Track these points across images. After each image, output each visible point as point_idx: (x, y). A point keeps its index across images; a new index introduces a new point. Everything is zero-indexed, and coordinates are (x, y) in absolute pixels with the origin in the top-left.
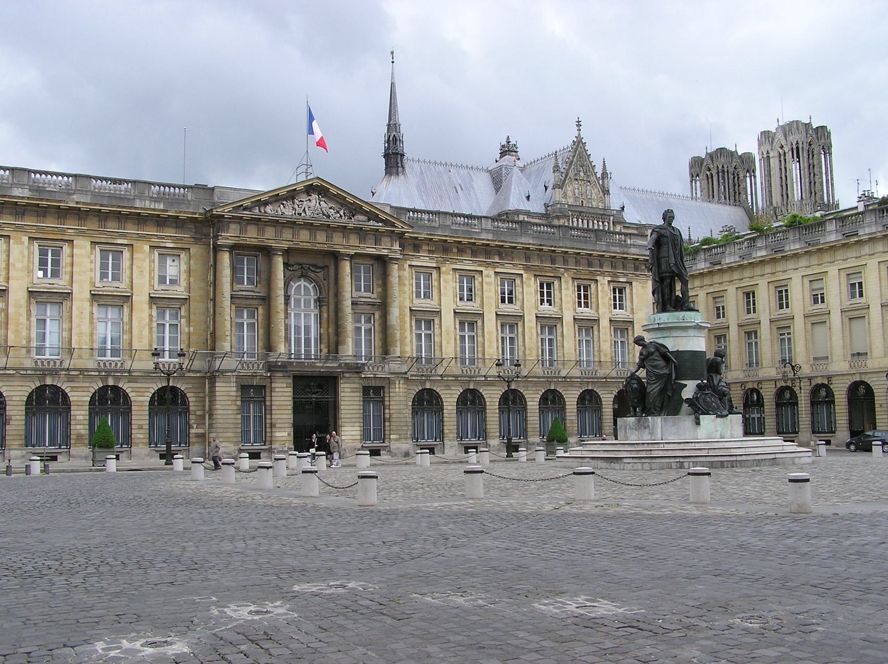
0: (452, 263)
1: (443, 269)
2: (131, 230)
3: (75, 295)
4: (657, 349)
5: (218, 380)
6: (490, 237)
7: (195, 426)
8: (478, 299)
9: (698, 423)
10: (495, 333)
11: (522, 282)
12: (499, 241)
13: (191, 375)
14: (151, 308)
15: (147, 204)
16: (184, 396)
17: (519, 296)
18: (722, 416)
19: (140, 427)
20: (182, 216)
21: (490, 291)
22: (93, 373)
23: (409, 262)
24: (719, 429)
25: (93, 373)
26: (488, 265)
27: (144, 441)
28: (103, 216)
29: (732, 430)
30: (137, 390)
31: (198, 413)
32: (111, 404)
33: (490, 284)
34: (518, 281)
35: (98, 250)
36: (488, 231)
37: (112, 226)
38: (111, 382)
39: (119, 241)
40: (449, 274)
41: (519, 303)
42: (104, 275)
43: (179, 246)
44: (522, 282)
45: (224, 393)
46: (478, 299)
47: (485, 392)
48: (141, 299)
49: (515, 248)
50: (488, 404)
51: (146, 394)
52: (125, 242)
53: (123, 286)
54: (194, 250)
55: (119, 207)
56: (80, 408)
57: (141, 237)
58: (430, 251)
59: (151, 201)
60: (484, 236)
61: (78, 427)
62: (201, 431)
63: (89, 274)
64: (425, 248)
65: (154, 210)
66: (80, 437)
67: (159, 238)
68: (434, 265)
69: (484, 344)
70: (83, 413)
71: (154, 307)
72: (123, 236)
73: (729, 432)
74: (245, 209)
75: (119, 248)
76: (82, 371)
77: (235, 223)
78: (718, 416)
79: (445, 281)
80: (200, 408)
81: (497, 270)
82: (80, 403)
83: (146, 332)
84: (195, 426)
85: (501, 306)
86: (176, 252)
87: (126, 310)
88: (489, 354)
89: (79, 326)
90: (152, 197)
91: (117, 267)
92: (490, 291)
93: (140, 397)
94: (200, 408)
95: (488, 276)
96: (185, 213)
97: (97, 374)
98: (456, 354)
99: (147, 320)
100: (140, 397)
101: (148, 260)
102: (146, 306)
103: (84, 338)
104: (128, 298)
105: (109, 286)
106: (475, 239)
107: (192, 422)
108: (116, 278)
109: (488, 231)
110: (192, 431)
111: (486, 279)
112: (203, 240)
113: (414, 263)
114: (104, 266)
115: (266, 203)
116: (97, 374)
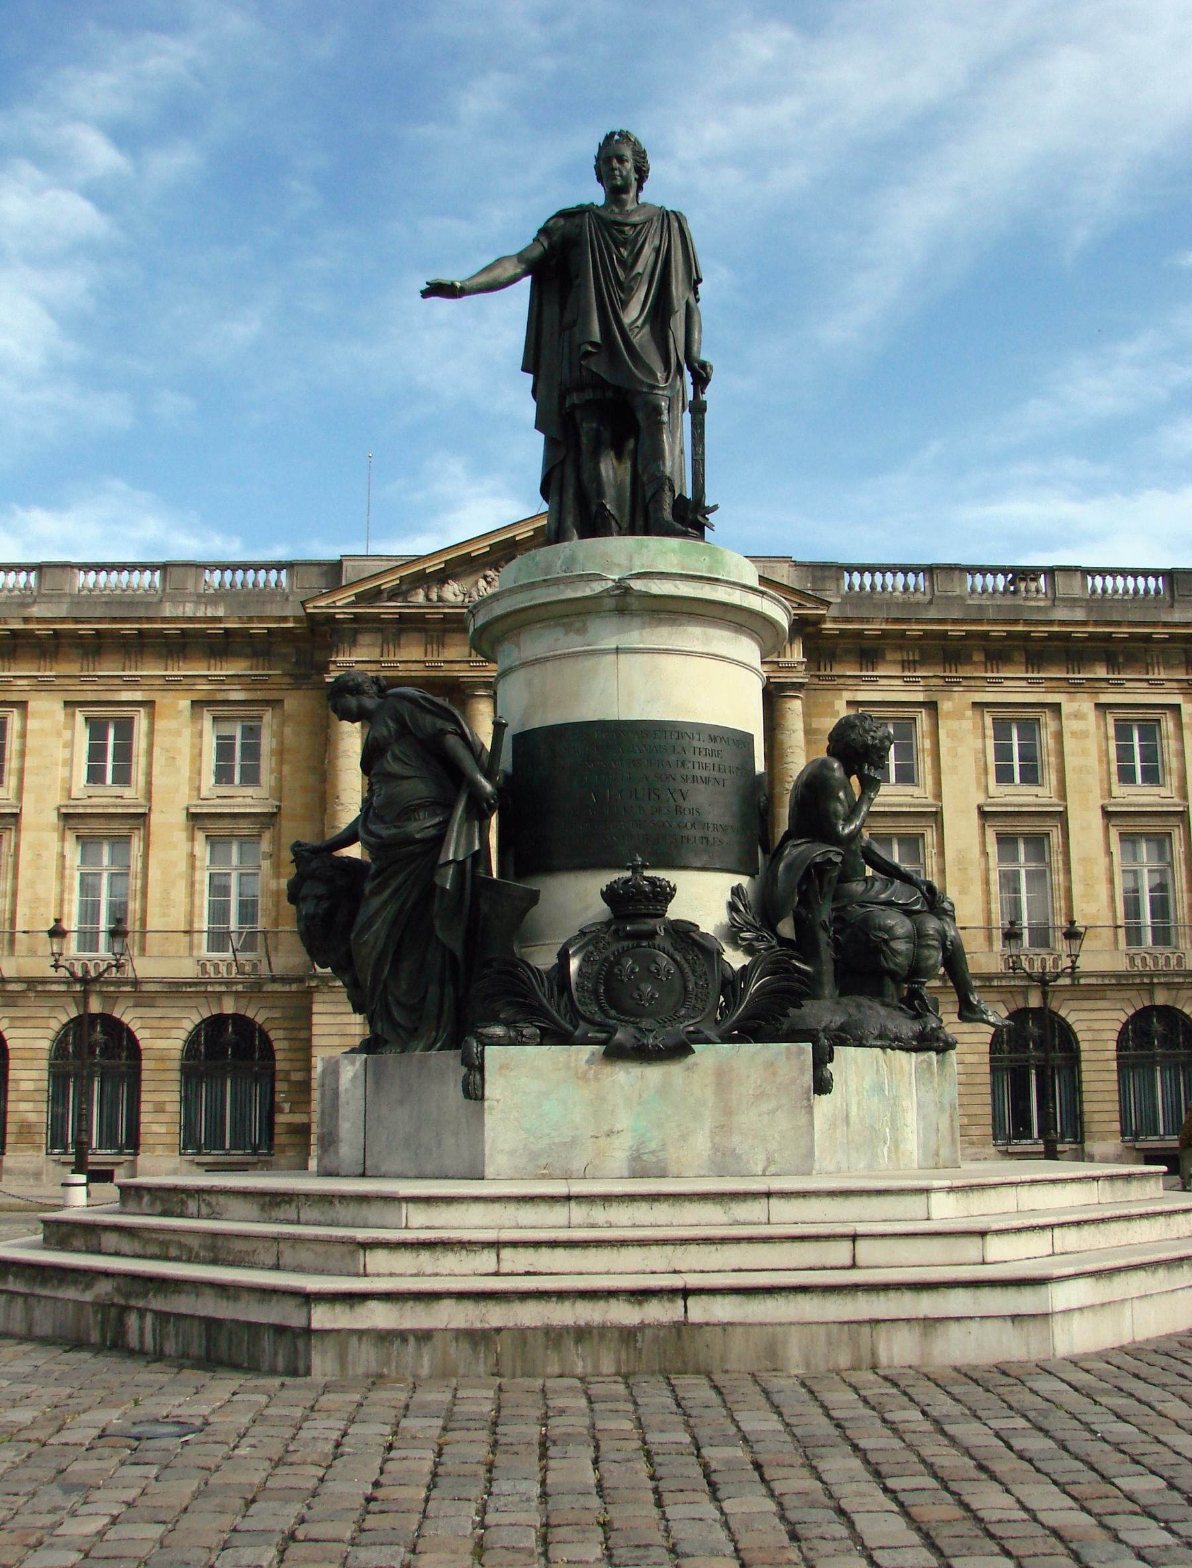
0: (969, 689)
1: (945, 706)
2: (152, 669)
3: (25, 819)
4: (404, 731)
5: (317, 997)
6: (1080, 615)
7: (287, 1107)
8: (1051, 778)
9: (474, 1092)
10: (1103, 861)
11: (1179, 726)
12: (1097, 623)
13: (278, 987)
14: (192, 839)
15: (189, 610)
16: (264, 1035)
17: (1174, 763)
18: (643, 1054)
19: (159, 1109)
20: (258, 627)
21: (1084, 752)
22: (55, 987)
23: (847, 696)
24: (624, 1120)
25: (55, 987)
26: (1074, 687)
27: (168, 1139)
28: (96, 645)
29: (723, 1128)
30: (155, 1023)
31: (295, 1076)
32: (102, 1055)
33: (1084, 735)
34: (1168, 725)
35: (80, 718)
36: (1073, 602)
37: (108, 668)
38: (95, 1006)
39: (126, 696)
40: (961, 716)
41: (1173, 781)
42: (95, 775)
43: (259, 695)
44: (1179, 726)
45: (333, 1030)
46: (1051, 778)
47: (1076, 1016)
48: (168, 820)
49: (1147, 638)
50: (1083, 1046)
51: (175, 1033)
52: (138, 696)
53: (132, 794)
54: (293, 702)
55: (114, 620)
56: (28, 1064)
57: (171, 684)
58: (905, 664)
59: (197, 603)
60: (1060, 614)
61: (23, 1106)
62: (299, 1118)
63: (61, 772)
64: (890, 656)
65: (190, 619)
66: (26, 1129)
67: (211, 682)
68: (920, 697)
69: (1069, 890)
70: (35, 1075)
71: (200, 836)
72: (132, 683)
73: (701, 1143)
74: (394, 594)
75: (125, 712)
76: (32, 983)
77: (368, 630)
78: (615, 1054)
79: (952, 735)
80: (299, 1065)
81: (1104, 699)
82: (28, 1054)
83: (180, 893)
84: (287, 1107)
85: (1118, 790)
86: (253, 710)
87: (136, 846)
88: (1084, 916)
89: (32, 884)
90: (199, 596)
91: (124, 753)
92: (1084, 752)
93: (163, 1038)
94: (299, 1065)
95: (1077, 716)
96: (261, 619)
97: (63, 988)
98: (989, 919)
99: (183, 866)
100: (163, 1038)
101: (187, 732)
102: (180, 836)
103: (42, 910)
104: (141, 819)
105: (108, 797)
106: (1027, 622)
107: (279, 1097)
108: (123, 776)
109: (1073, 602)
110: (280, 1119)
111: (1069, 725)
112: (315, 678)
113: (861, 696)
114: (97, 753)
115: (442, 577)
116: (63, 988)
